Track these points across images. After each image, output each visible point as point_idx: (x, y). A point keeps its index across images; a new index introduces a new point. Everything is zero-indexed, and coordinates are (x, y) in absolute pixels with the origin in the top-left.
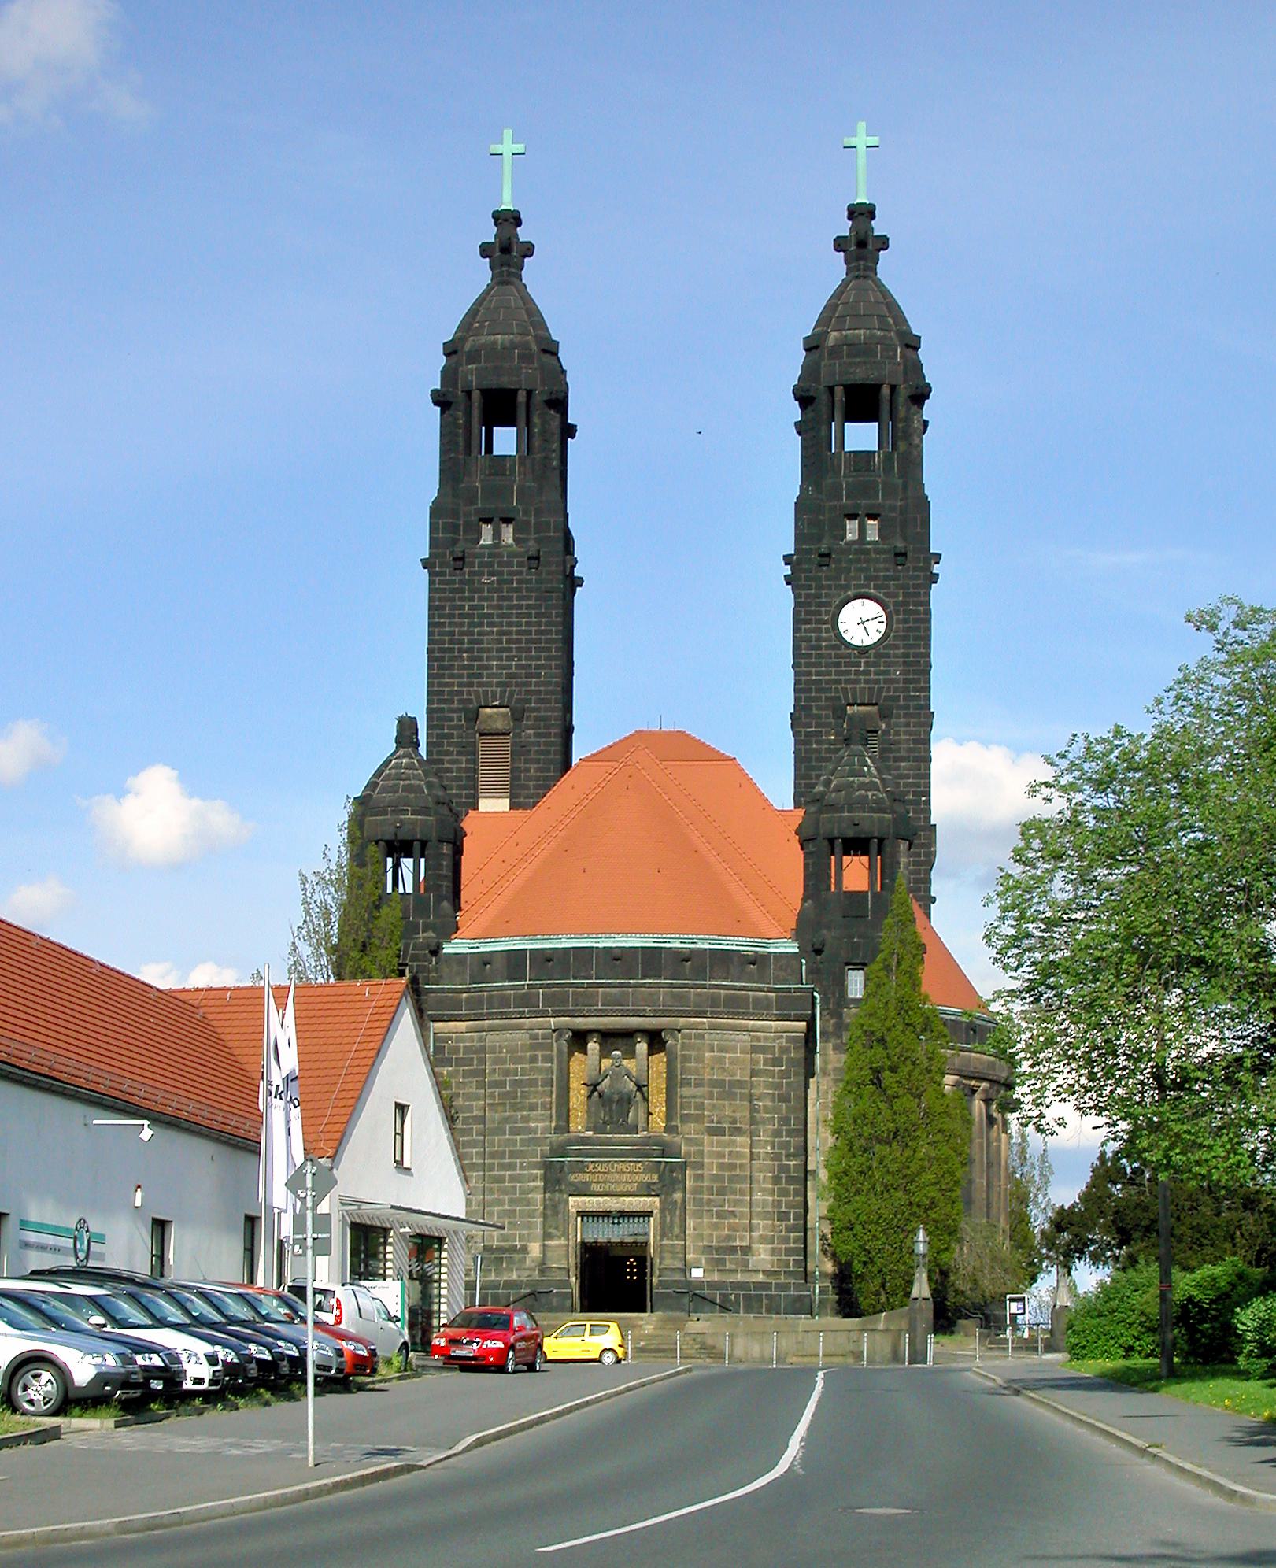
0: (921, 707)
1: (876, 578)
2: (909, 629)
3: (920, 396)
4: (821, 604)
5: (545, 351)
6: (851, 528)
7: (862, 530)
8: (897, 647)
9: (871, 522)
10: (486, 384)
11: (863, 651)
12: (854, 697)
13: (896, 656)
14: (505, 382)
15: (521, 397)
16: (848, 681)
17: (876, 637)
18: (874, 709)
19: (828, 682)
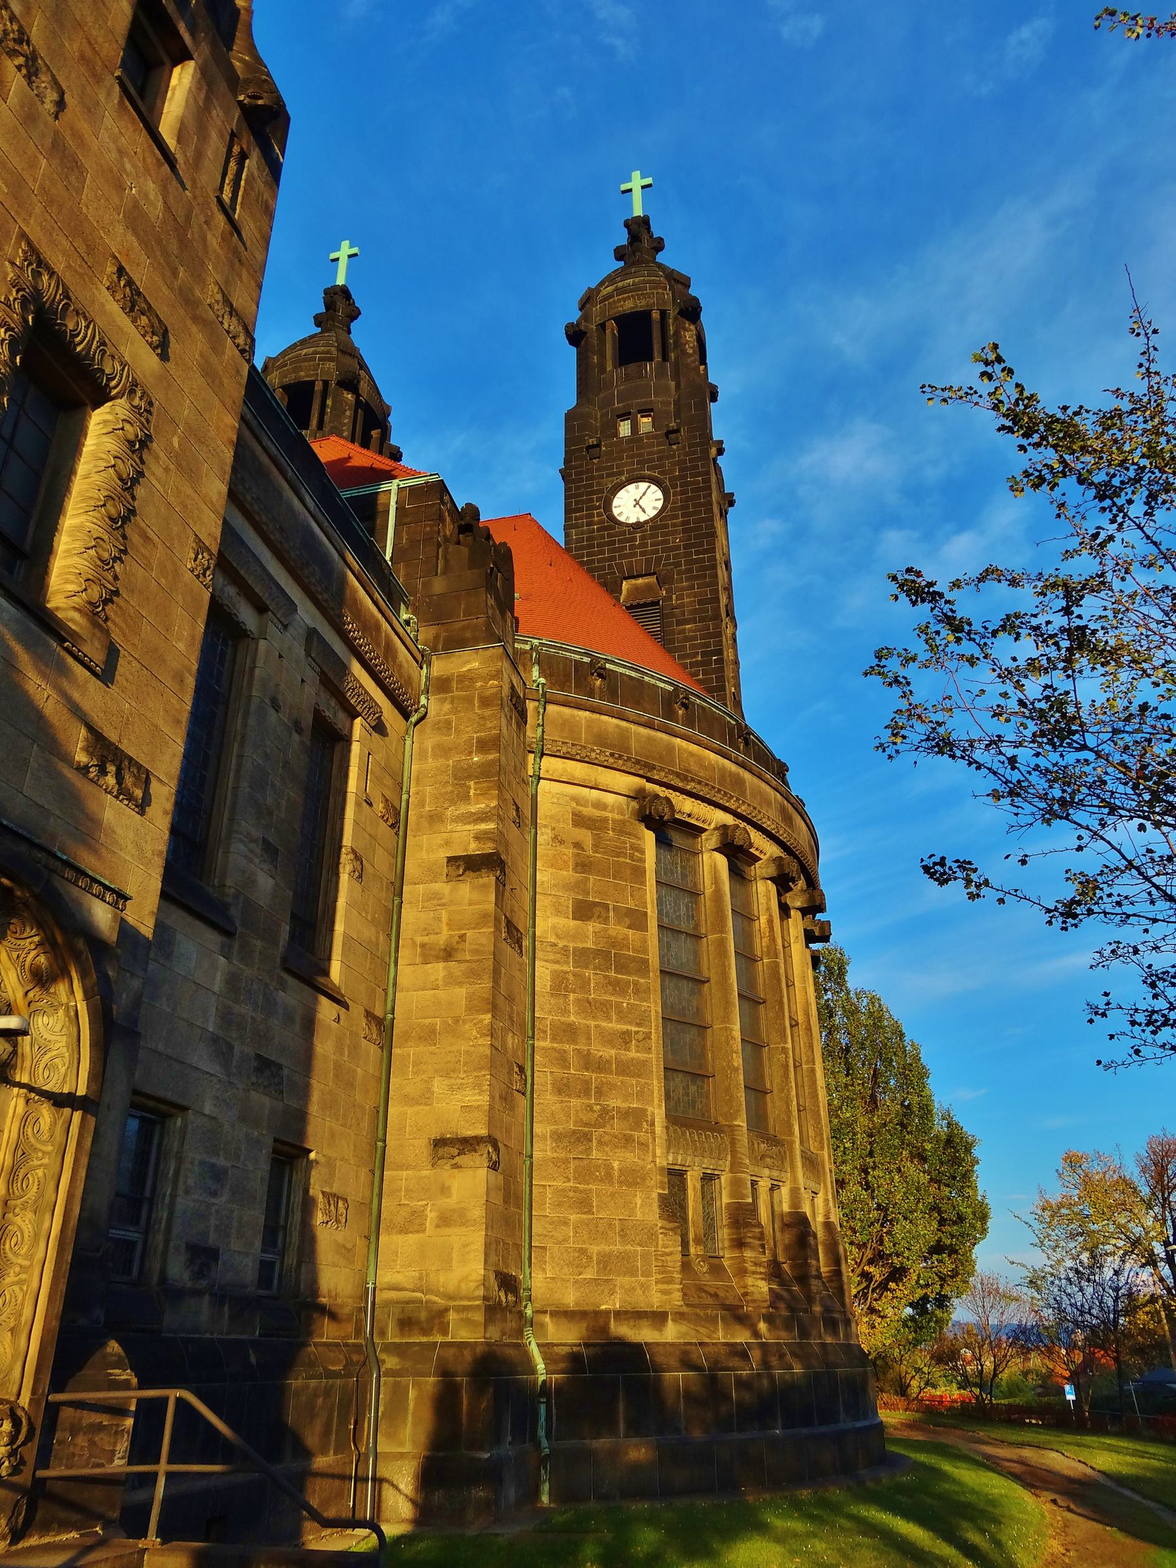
0: (704, 568)
1: (653, 460)
2: (688, 499)
3: (692, 312)
4: (593, 493)
5: (344, 352)
6: (625, 429)
7: (635, 427)
8: (676, 517)
9: (645, 420)
10: (286, 381)
11: (638, 525)
12: (630, 568)
13: (674, 525)
14: (304, 376)
15: (319, 386)
16: (622, 557)
17: (653, 513)
18: (653, 579)
19: (599, 561)
